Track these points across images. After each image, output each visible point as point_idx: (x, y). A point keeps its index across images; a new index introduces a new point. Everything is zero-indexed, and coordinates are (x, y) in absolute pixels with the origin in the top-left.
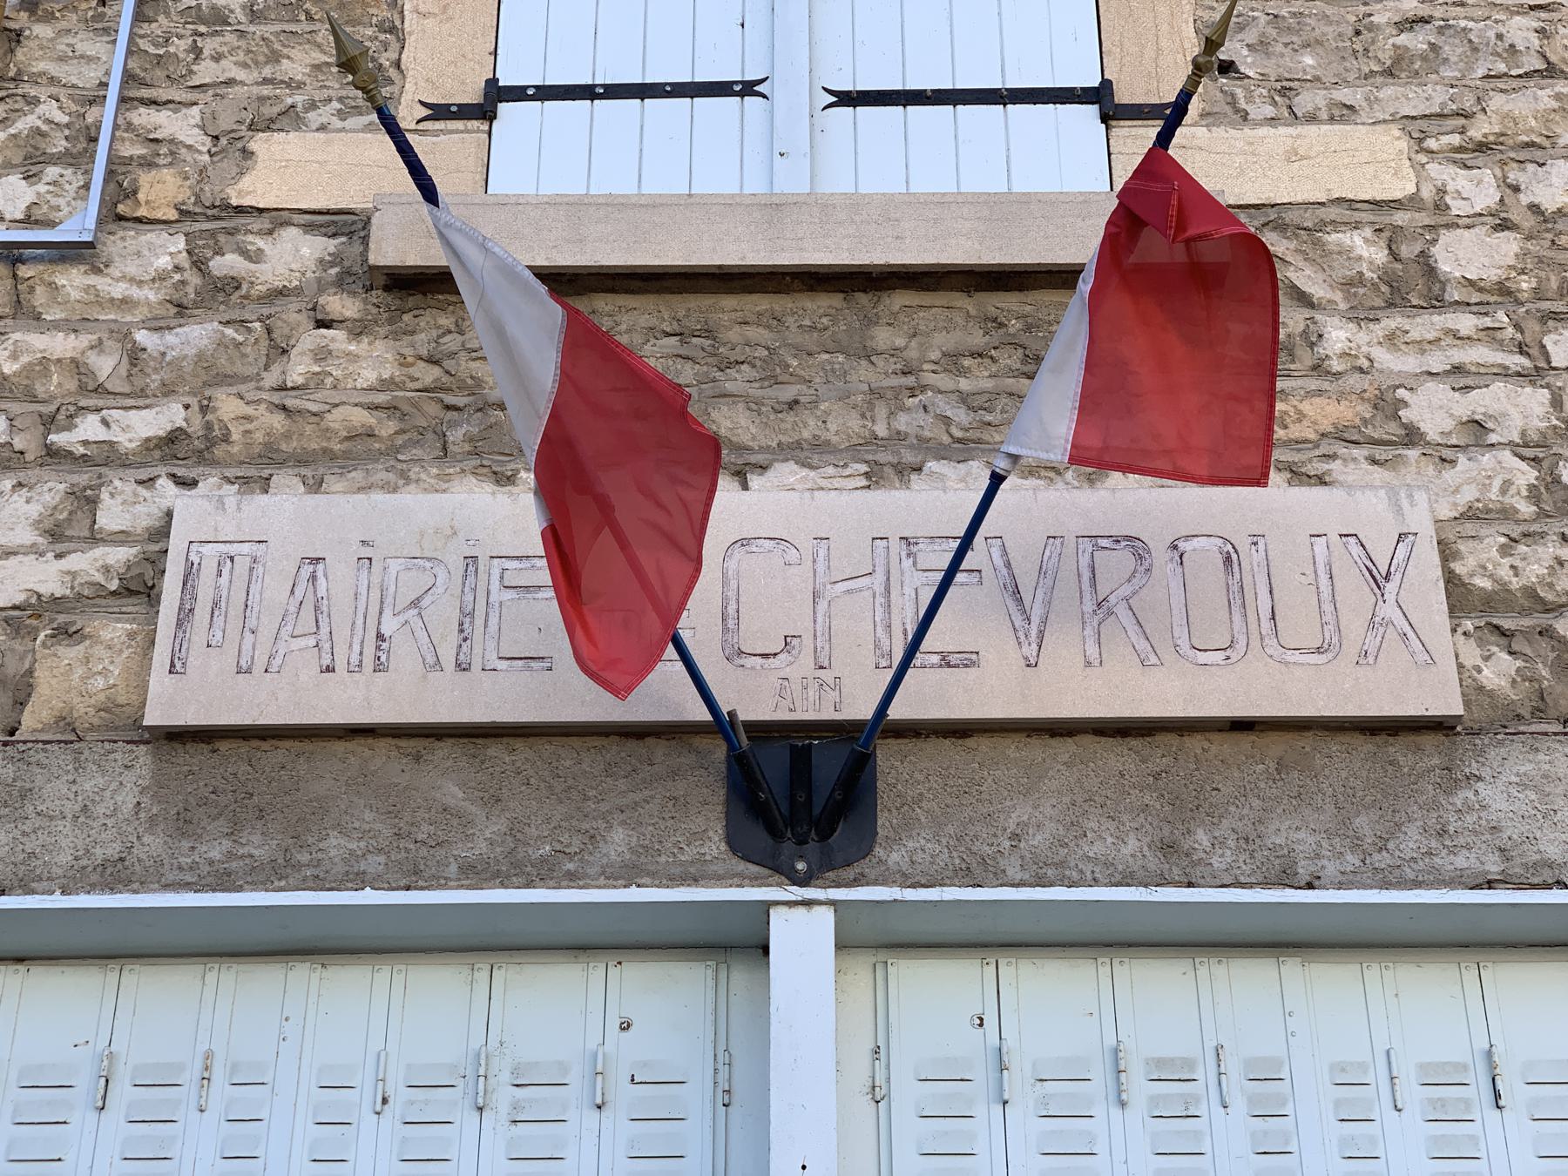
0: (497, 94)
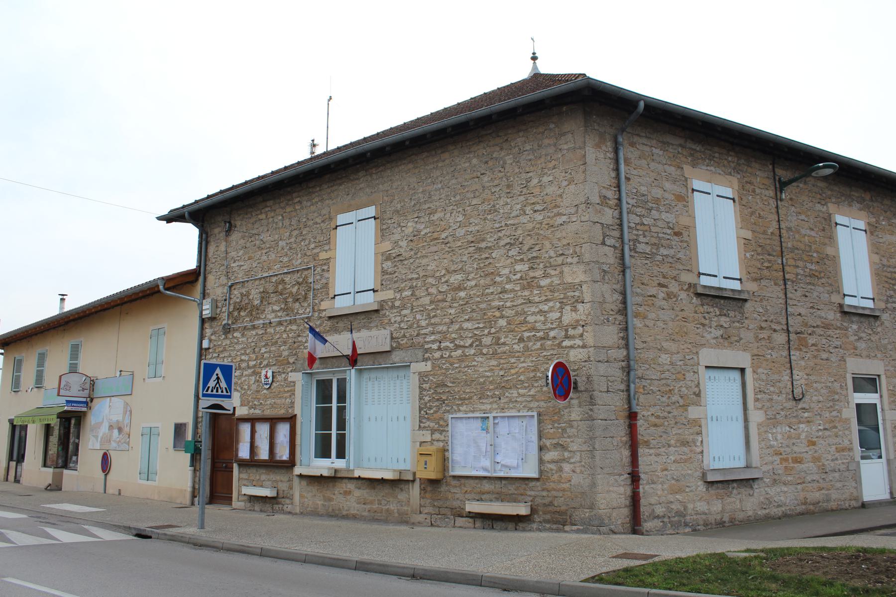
0: (335, 296)
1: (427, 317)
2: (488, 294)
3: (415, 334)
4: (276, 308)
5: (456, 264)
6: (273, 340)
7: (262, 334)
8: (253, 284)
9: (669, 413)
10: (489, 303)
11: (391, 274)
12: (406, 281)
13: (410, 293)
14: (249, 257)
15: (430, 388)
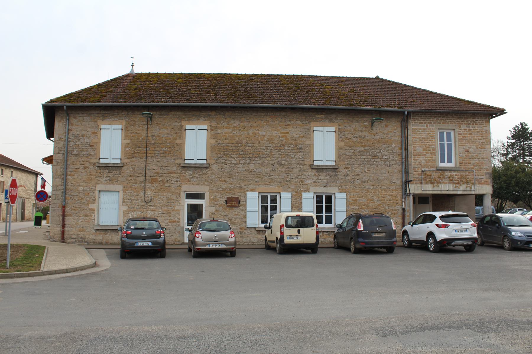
9: (81, 206)
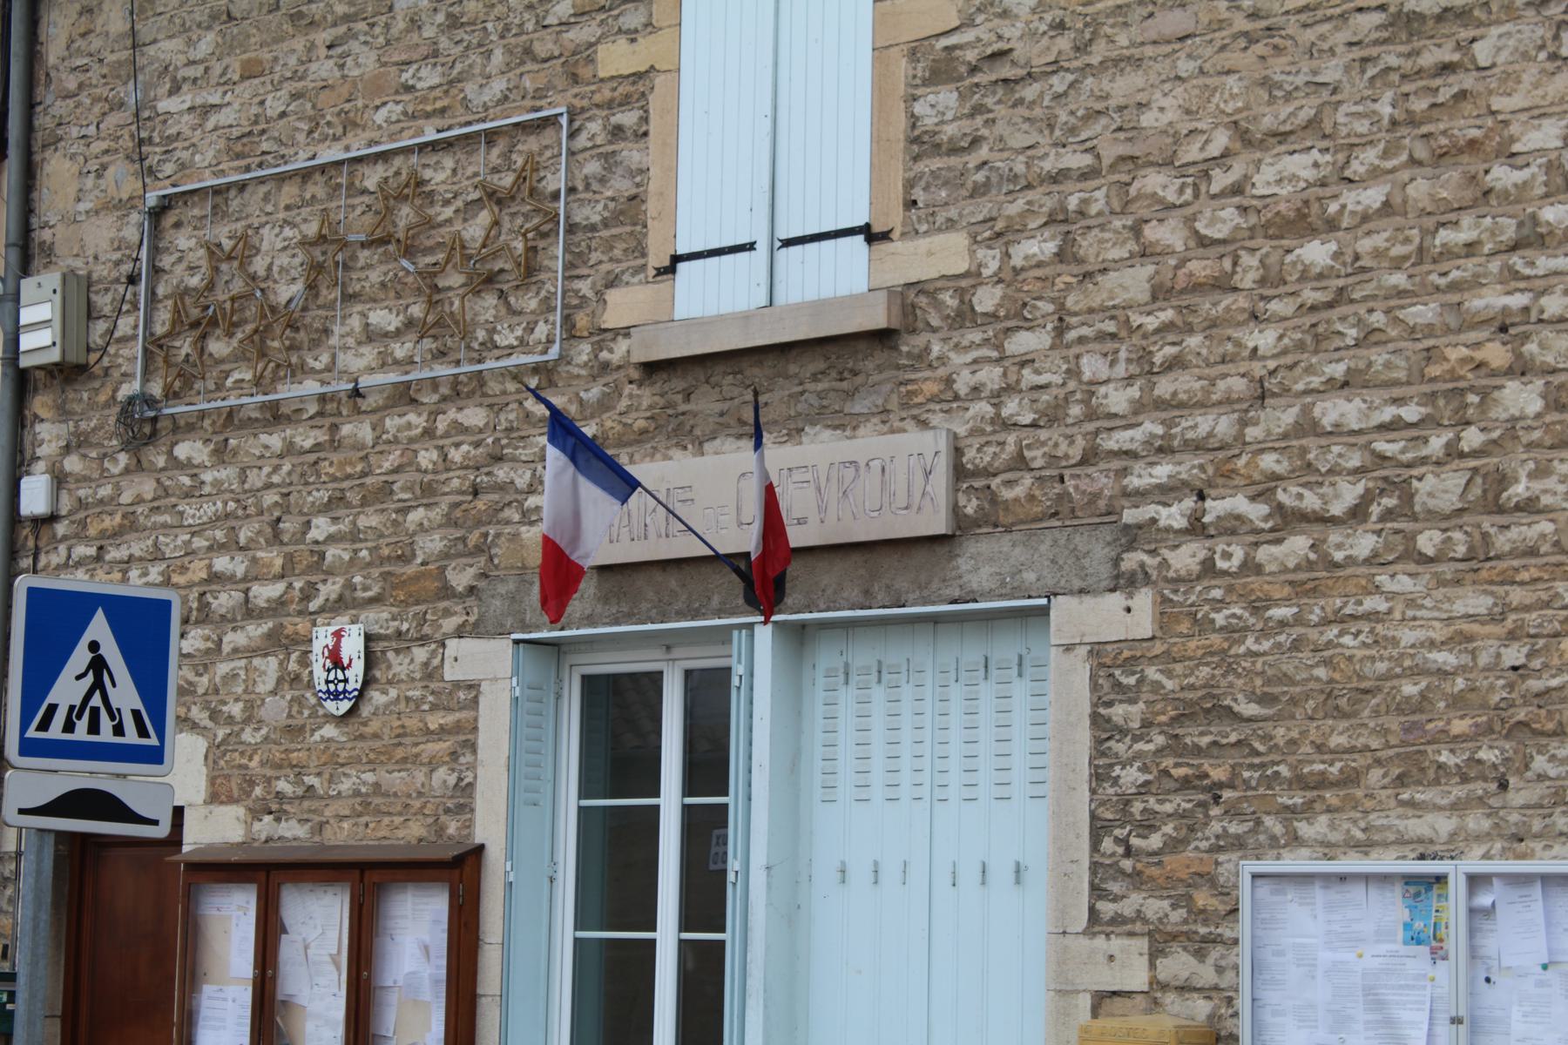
0: (677, 259)
1: (1135, 369)
2: (1447, 253)
3: (1076, 453)
4: (385, 318)
5: (1288, 97)
6: (369, 480)
7: (317, 447)
8: (266, 198)
10: (1455, 298)
11: (954, 150)
12: (1029, 187)
13: (1051, 247)
14: (246, 65)
15: (1147, 724)
